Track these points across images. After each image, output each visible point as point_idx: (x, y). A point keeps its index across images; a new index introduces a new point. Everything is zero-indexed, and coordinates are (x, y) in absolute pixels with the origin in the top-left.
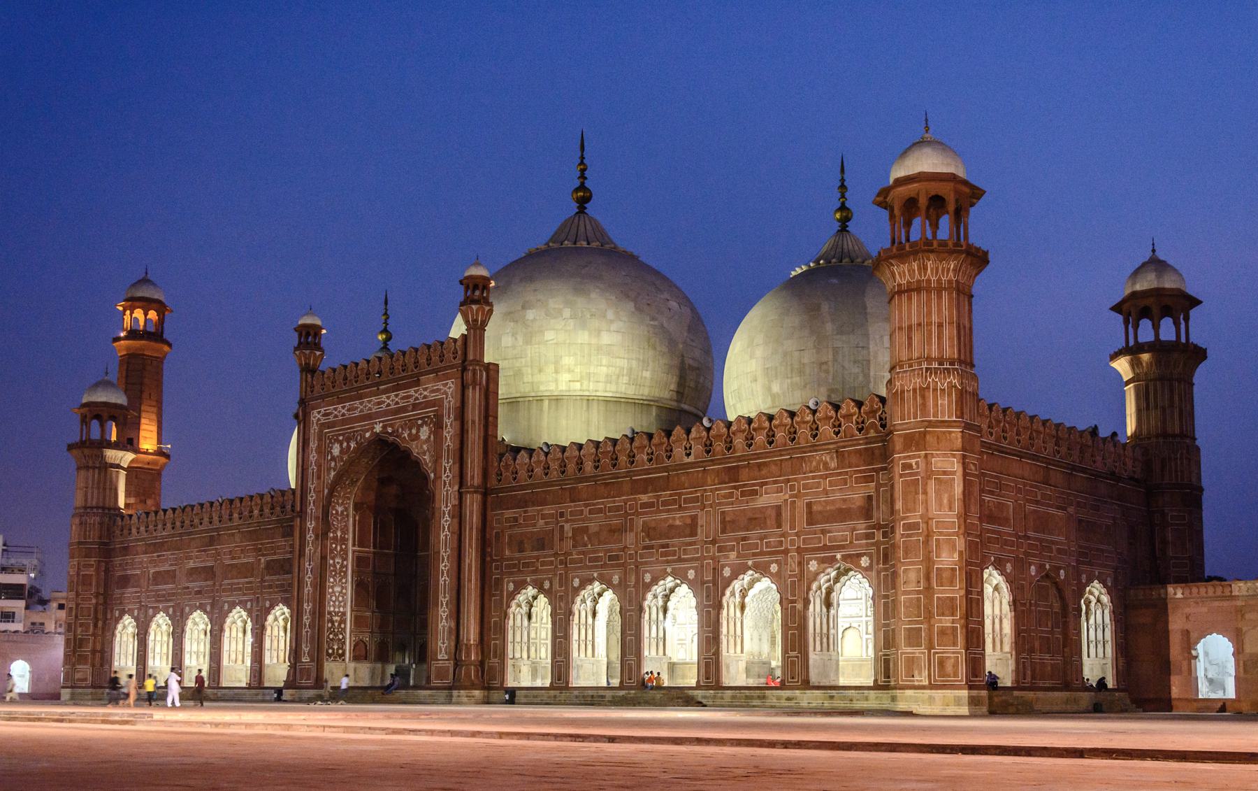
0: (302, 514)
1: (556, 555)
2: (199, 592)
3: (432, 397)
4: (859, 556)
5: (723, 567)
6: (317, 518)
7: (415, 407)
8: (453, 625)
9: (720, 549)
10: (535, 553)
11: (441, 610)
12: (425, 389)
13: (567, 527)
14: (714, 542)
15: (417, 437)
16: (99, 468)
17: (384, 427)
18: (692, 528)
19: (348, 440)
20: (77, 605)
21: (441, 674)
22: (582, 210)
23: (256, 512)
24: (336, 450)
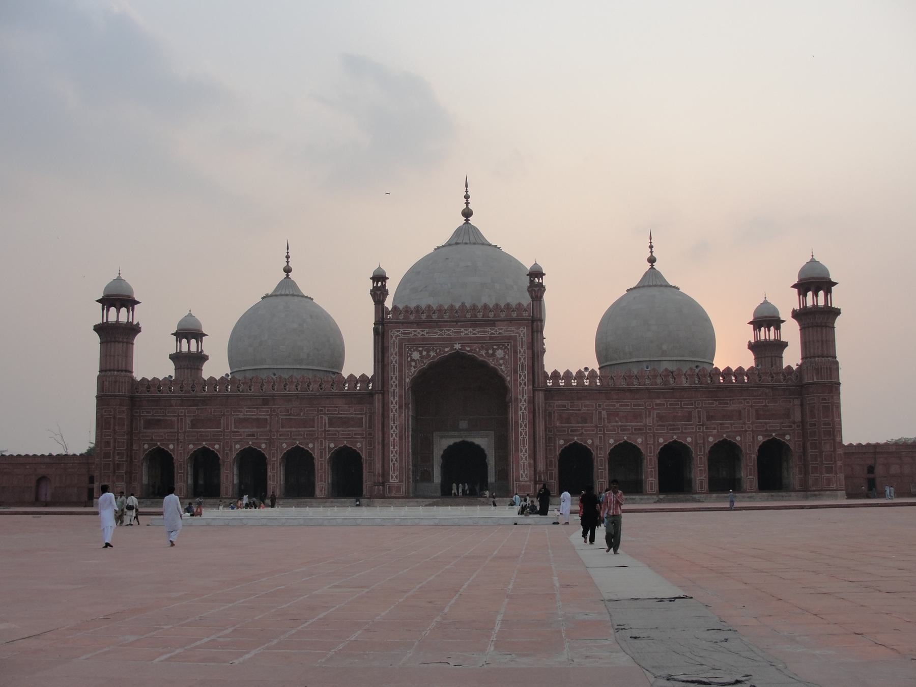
0: (384, 392)
1: (596, 426)
2: (253, 435)
3: (506, 334)
4: (785, 435)
5: (708, 436)
6: (400, 397)
7: (491, 338)
8: (532, 462)
9: (707, 428)
13: (604, 413)
15: (493, 355)
16: (127, 343)
17: (463, 345)
18: (689, 418)
20: (115, 440)
21: (522, 488)
22: (467, 220)
23: (317, 386)
24: (416, 355)
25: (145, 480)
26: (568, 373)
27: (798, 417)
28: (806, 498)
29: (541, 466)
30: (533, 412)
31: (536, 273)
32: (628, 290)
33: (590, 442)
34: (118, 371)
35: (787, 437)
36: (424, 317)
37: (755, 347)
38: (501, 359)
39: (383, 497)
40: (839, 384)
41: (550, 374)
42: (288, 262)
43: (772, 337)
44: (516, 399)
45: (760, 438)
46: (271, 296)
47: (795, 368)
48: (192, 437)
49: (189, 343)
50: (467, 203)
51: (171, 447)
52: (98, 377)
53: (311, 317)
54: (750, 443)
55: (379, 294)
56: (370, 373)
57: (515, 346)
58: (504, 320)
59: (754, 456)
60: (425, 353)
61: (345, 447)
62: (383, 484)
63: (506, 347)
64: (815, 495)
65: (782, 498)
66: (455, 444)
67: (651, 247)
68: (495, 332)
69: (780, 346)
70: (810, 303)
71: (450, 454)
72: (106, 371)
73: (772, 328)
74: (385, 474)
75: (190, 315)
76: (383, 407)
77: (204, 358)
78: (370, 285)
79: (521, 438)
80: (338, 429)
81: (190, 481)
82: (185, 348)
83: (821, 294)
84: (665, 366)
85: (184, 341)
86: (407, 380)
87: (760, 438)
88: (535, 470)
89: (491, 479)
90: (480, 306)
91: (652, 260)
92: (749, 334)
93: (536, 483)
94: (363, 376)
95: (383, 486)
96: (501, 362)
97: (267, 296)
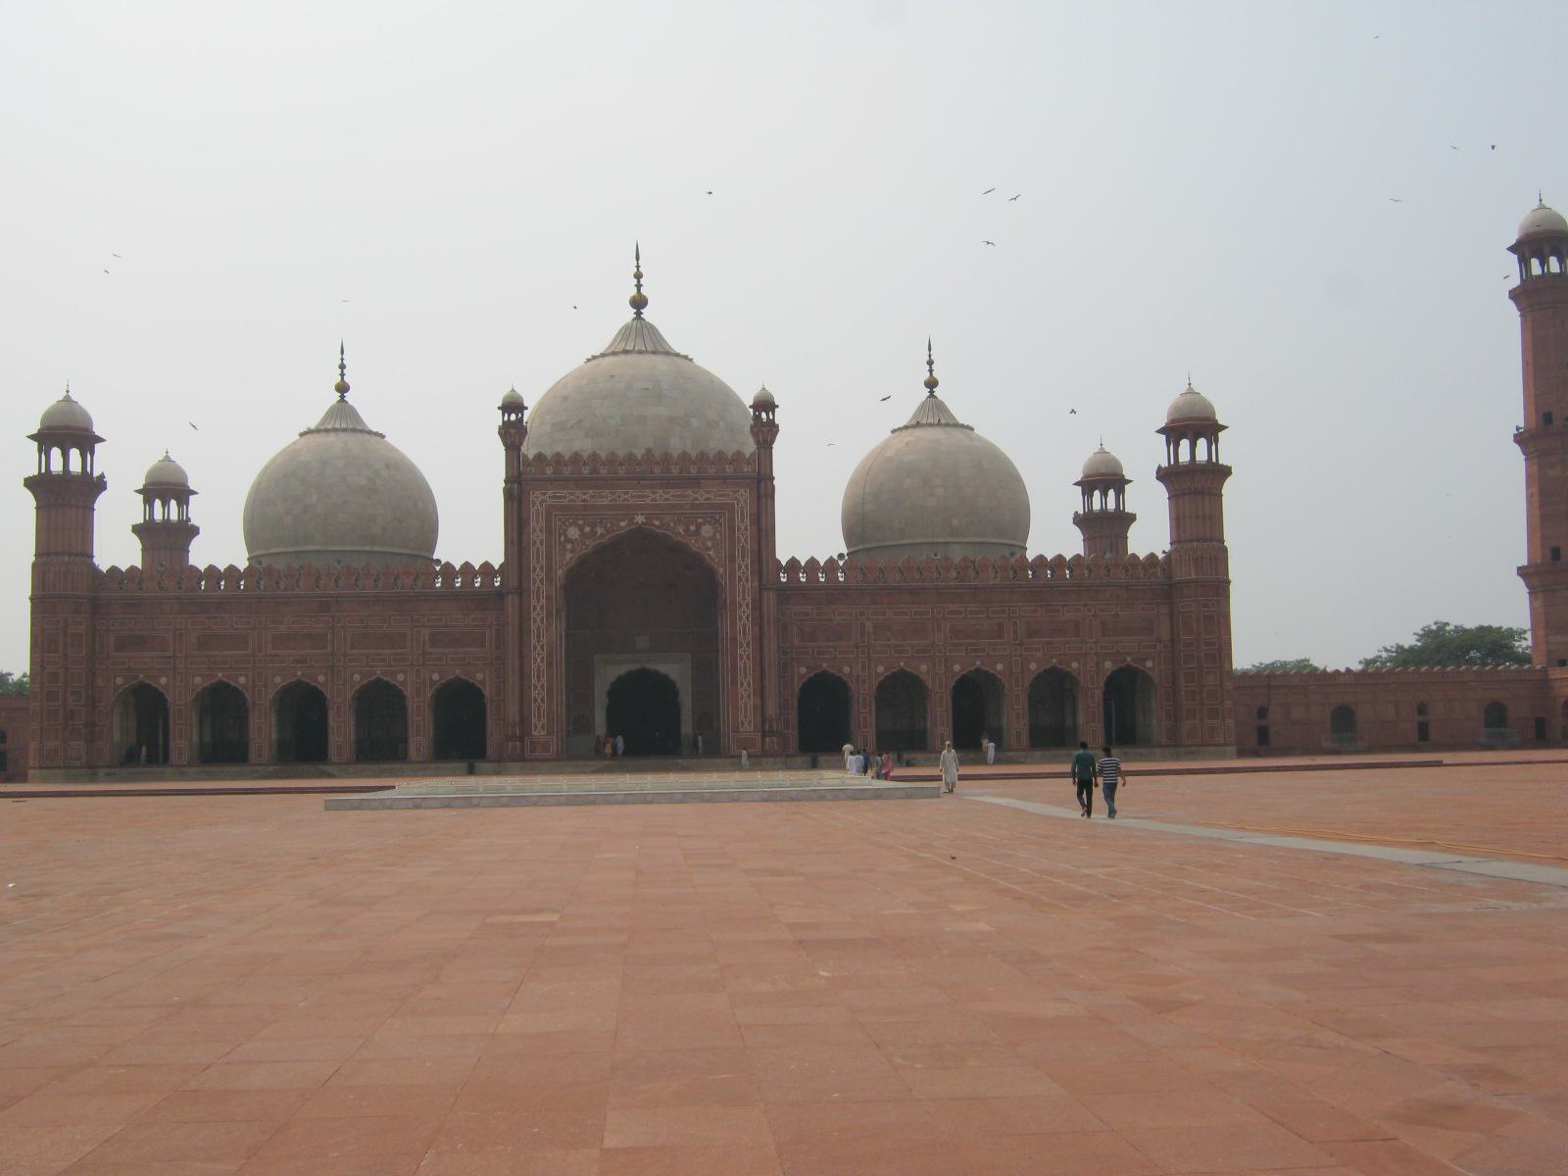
0: (521, 591)
1: (857, 647)
3: (719, 500)
4: (1145, 660)
6: (549, 598)
7: (693, 506)
8: (759, 701)
10: (830, 644)
11: (740, 690)
12: (709, 492)
13: (869, 625)
14: (1021, 644)
15: (697, 532)
19: (593, 526)
22: (638, 314)
24: (573, 533)
25: (117, 737)
26: (812, 561)
27: (1166, 635)
28: (1177, 758)
29: (772, 710)
30: (759, 620)
31: (765, 404)
32: (894, 431)
33: (847, 670)
34: (70, 554)
35: (1149, 664)
36: (586, 471)
37: (1086, 522)
38: (710, 539)
39: (522, 759)
40: (1229, 582)
41: (784, 563)
42: (342, 375)
43: (1111, 505)
44: (733, 602)
45: (1108, 665)
46: (317, 431)
47: (1161, 556)
48: (250, 665)
49: (165, 504)
50: (639, 286)
51: (163, 680)
52: (34, 565)
53: (387, 466)
54: (1092, 672)
55: (512, 434)
56: (497, 559)
57: (732, 519)
58: (713, 478)
59: (1099, 693)
60: (587, 529)
61: (458, 679)
62: (521, 739)
63: (717, 521)
64: (1193, 753)
65: (1142, 758)
66: (629, 674)
67: (930, 363)
68: (701, 496)
69: (1124, 520)
70: (1184, 456)
71: (621, 691)
72: (48, 554)
73: (1111, 493)
74: (524, 722)
75: (167, 459)
76: (521, 617)
77: (195, 531)
78: (497, 419)
79: (740, 664)
80: (446, 650)
81: (195, 738)
82: (158, 516)
83: (1202, 443)
84: (957, 555)
85: (158, 503)
86: (560, 572)
87: (1108, 665)
88: (763, 715)
89: (687, 727)
90: (675, 456)
91: (931, 384)
92: (1075, 502)
93: (764, 736)
94: (486, 566)
95: (523, 741)
96: (709, 544)
97: (309, 432)
